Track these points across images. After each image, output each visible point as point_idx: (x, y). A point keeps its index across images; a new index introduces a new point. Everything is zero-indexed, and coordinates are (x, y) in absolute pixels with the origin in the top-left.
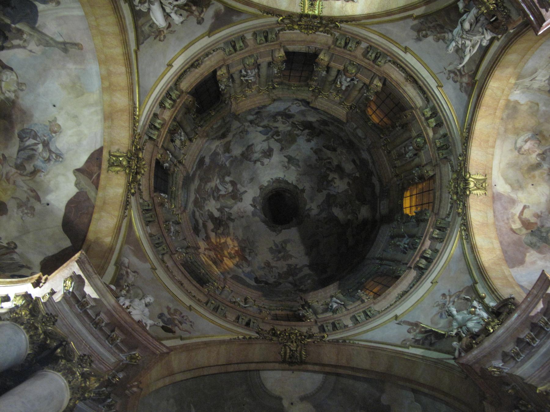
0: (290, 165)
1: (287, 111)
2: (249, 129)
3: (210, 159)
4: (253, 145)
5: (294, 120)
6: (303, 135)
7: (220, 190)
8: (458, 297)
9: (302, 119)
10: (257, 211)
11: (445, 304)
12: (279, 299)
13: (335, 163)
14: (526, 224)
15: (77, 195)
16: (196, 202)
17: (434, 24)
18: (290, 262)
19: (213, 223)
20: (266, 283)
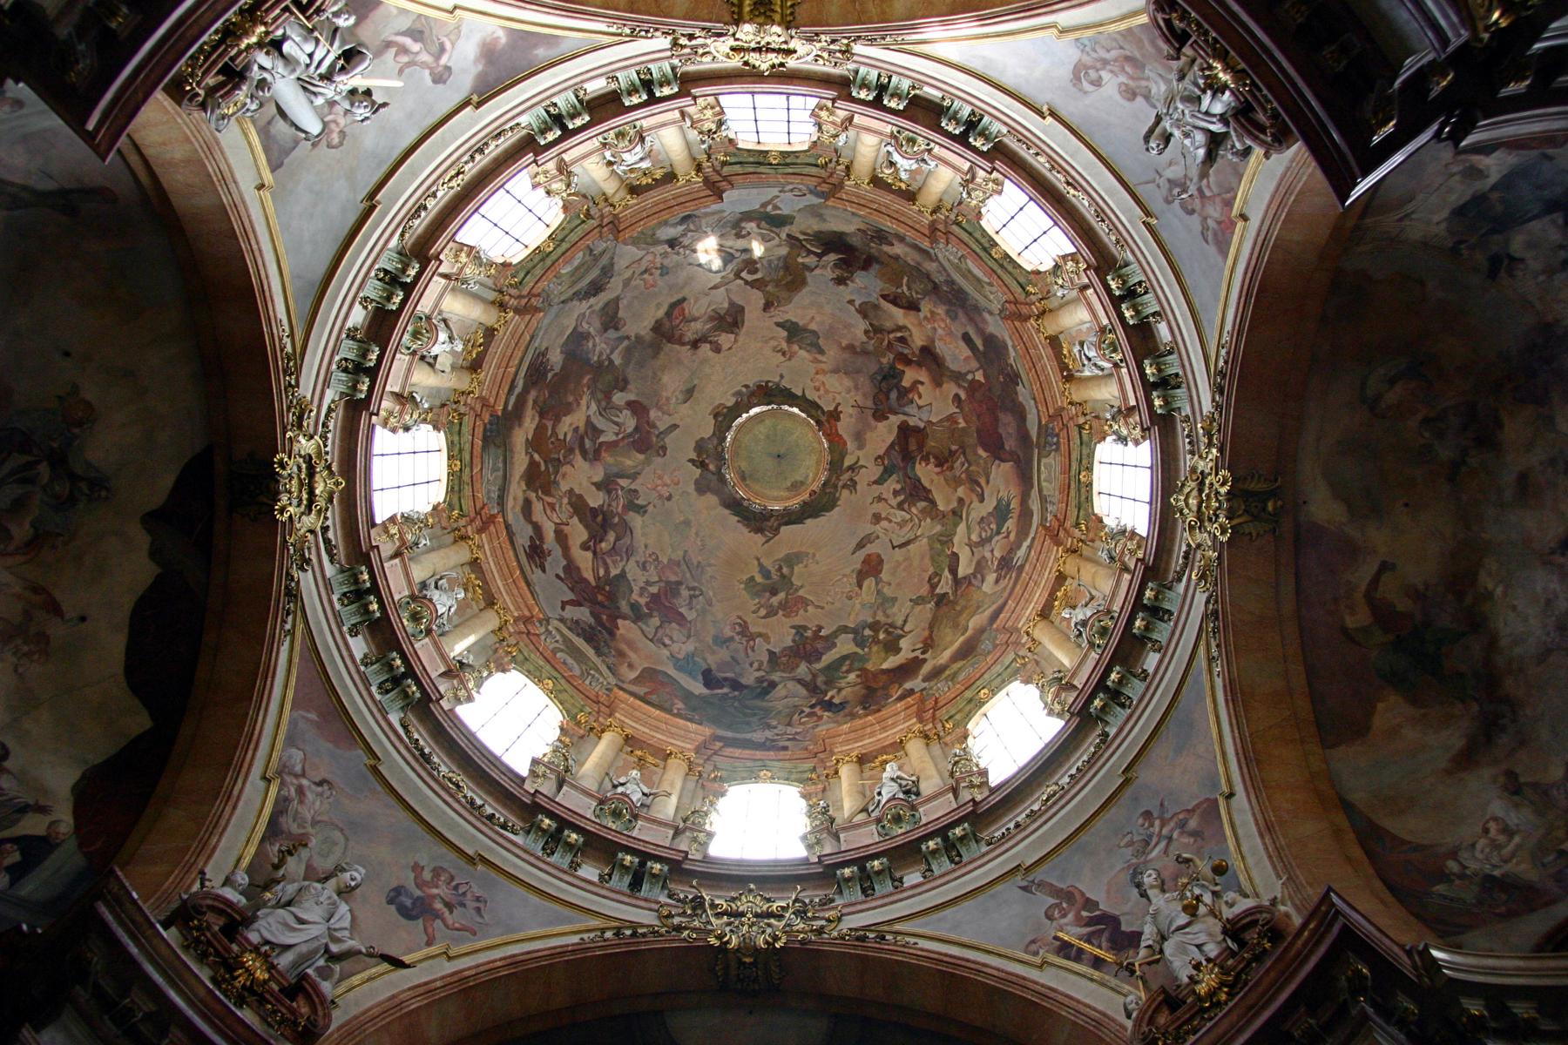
0: (796, 347)
1: (769, 208)
2: (666, 262)
4: (684, 299)
5: (794, 229)
6: (824, 267)
8: (1182, 825)
9: (816, 228)
10: (710, 476)
12: (768, 734)
13: (918, 340)
14: (1383, 614)
15: (157, 585)
16: (534, 478)
17: (1114, 53)
19: (587, 527)
20: (736, 685)
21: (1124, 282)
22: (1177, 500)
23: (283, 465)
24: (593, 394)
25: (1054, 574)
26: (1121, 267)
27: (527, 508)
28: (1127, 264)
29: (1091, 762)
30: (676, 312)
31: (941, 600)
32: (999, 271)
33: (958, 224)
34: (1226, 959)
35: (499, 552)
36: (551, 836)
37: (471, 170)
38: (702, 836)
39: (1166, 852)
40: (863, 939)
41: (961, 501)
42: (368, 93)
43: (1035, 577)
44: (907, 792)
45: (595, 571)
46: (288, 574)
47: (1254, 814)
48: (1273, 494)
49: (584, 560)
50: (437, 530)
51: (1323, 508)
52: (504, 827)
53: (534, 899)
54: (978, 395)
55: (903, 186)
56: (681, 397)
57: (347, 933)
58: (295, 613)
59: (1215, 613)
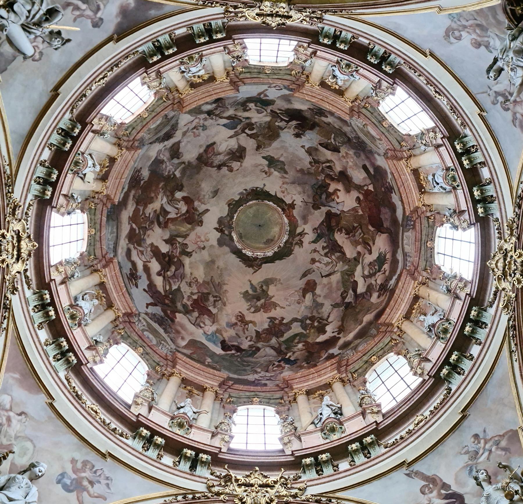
0: (272, 170)
1: (262, 96)
2: (206, 123)
3: (149, 170)
5: (274, 107)
6: (289, 128)
7: (169, 213)
8: (497, 444)
11: (477, 453)
12: (256, 376)
13: (338, 168)
16: (132, 237)
18: (273, 313)
19: (160, 263)
20: (238, 349)
21: (464, 145)
24: (164, 192)
26: (463, 137)
30: (210, 150)
31: (348, 306)
32: (386, 134)
33: (366, 108)
35: (115, 278)
36: (147, 440)
37: (111, 75)
41: (359, 253)
42: (59, 33)
44: (335, 413)
45: (164, 287)
46: (5, 296)
49: (159, 281)
50: (83, 268)
52: (121, 435)
54: (370, 198)
55: (337, 87)
56: (211, 195)
58: (9, 318)
59: (514, 327)
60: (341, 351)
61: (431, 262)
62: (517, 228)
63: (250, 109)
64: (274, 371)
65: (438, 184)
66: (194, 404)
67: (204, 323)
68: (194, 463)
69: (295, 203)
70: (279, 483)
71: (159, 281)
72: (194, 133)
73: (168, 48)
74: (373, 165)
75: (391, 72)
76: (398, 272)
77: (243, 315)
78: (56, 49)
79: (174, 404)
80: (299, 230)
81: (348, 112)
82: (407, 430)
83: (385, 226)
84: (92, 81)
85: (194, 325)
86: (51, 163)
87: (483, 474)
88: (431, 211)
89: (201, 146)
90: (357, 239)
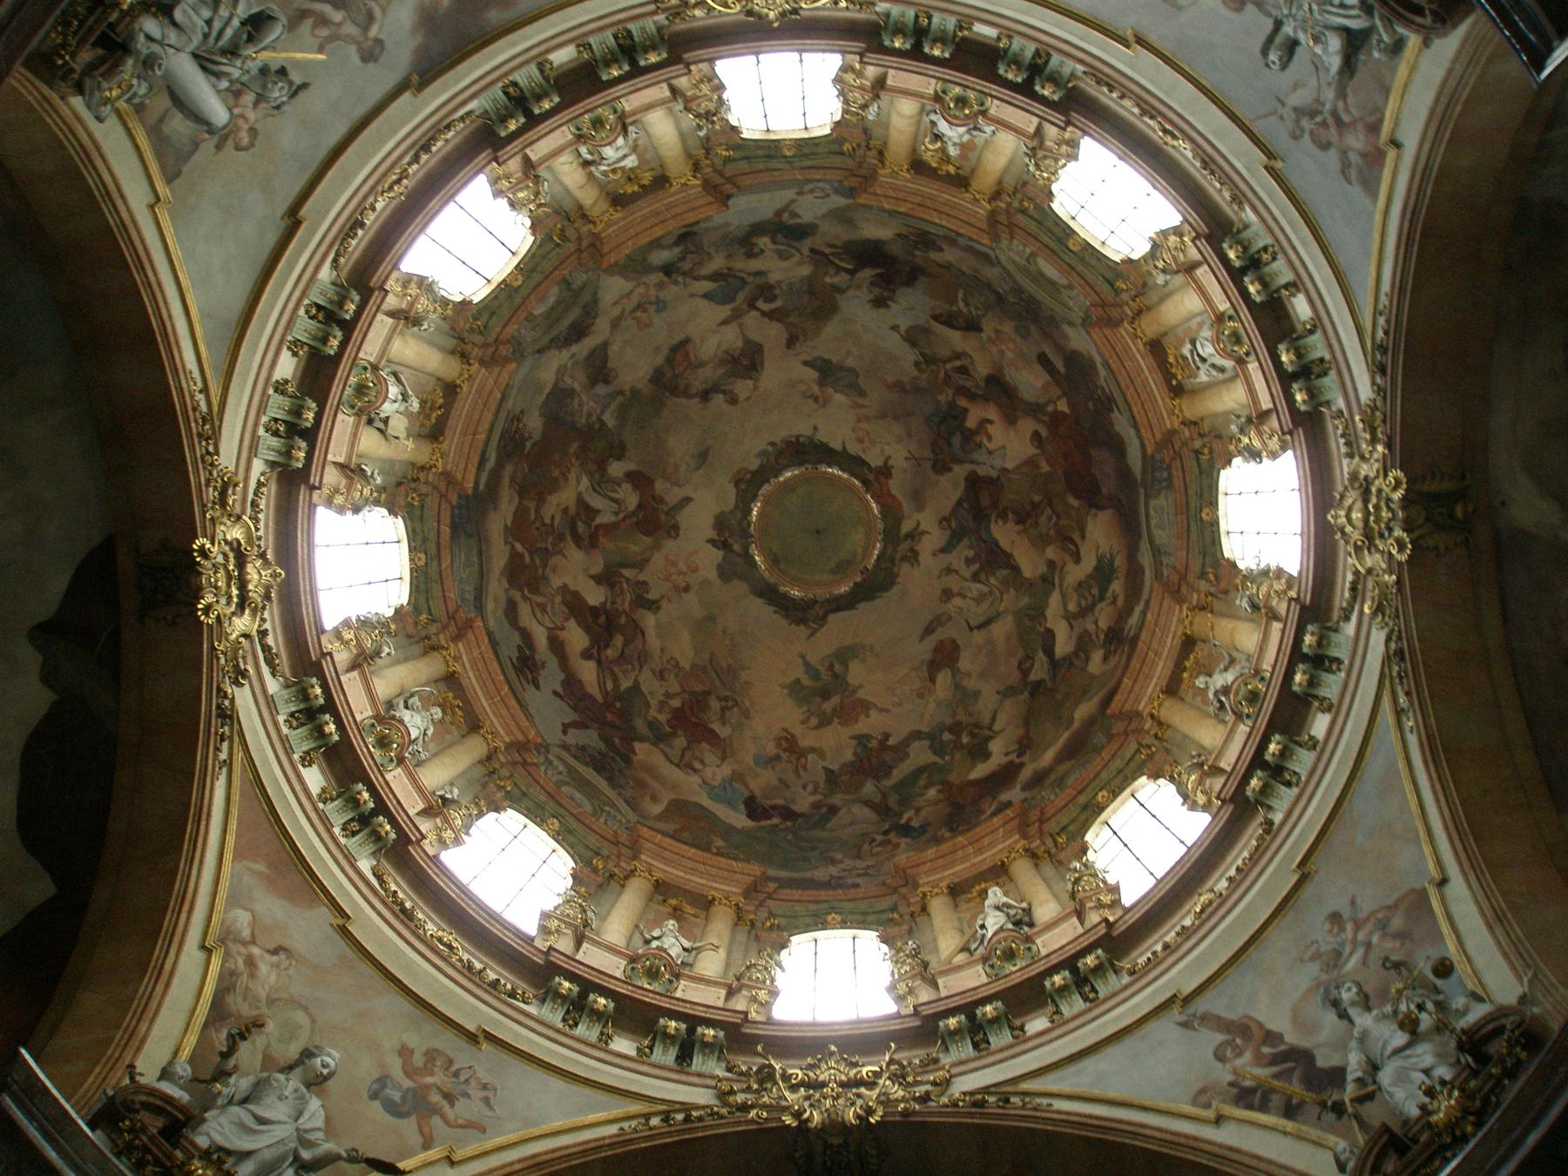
0: (830, 390)
1: (785, 216)
2: (663, 295)
4: (688, 340)
6: (858, 287)
7: (597, 512)
8: (1383, 926)
12: (833, 870)
13: (982, 369)
16: (517, 573)
18: (862, 727)
19: (587, 629)
20: (787, 814)
22: (1337, 517)
23: (204, 553)
24: (582, 465)
25: (1178, 642)
27: (511, 610)
28: (1246, 227)
29: (1254, 859)
31: (1036, 689)
32: (1080, 268)
33: (1023, 211)
34: (1467, 1080)
35: (481, 665)
36: (573, 1003)
38: (763, 995)
39: (1364, 963)
40: (981, 1104)
41: (1051, 564)
42: (282, 72)
43: (1154, 645)
45: (602, 685)
47: (1477, 902)
48: (1461, 495)
49: (588, 672)
51: (1528, 508)
52: (512, 995)
53: (557, 1084)
55: (952, 170)
57: (320, 1135)
59: (1400, 653)
60: (1027, 794)
61: (1214, 556)
62: (1384, 421)
63: (762, 251)
64: (873, 855)
65: (1203, 360)
66: (683, 930)
67: (702, 762)
68: (686, 1050)
69: (890, 463)
70: (885, 1075)
71: (588, 672)
72: (638, 321)
73: (539, 98)
74: (1060, 349)
75: (1056, 98)
76: (1145, 596)
77: (793, 736)
78: (278, 107)
79: (637, 935)
80: (906, 527)
81: (985, 226)
82: (1178, 928)
83: (1104, 491)
84: (373, 189)
85: (677, 766)
86: (300, 387)
87: (1349, 989)
88: (1201, 435)
89: (657, 349)
90: (1044, 531)
